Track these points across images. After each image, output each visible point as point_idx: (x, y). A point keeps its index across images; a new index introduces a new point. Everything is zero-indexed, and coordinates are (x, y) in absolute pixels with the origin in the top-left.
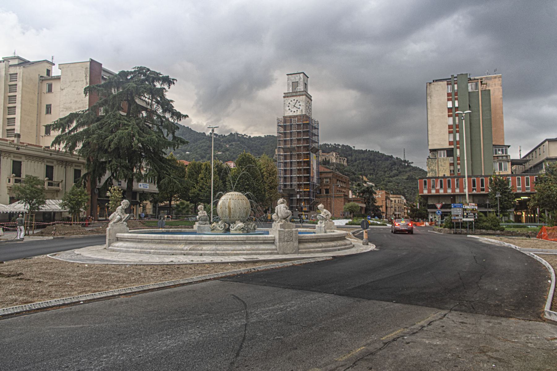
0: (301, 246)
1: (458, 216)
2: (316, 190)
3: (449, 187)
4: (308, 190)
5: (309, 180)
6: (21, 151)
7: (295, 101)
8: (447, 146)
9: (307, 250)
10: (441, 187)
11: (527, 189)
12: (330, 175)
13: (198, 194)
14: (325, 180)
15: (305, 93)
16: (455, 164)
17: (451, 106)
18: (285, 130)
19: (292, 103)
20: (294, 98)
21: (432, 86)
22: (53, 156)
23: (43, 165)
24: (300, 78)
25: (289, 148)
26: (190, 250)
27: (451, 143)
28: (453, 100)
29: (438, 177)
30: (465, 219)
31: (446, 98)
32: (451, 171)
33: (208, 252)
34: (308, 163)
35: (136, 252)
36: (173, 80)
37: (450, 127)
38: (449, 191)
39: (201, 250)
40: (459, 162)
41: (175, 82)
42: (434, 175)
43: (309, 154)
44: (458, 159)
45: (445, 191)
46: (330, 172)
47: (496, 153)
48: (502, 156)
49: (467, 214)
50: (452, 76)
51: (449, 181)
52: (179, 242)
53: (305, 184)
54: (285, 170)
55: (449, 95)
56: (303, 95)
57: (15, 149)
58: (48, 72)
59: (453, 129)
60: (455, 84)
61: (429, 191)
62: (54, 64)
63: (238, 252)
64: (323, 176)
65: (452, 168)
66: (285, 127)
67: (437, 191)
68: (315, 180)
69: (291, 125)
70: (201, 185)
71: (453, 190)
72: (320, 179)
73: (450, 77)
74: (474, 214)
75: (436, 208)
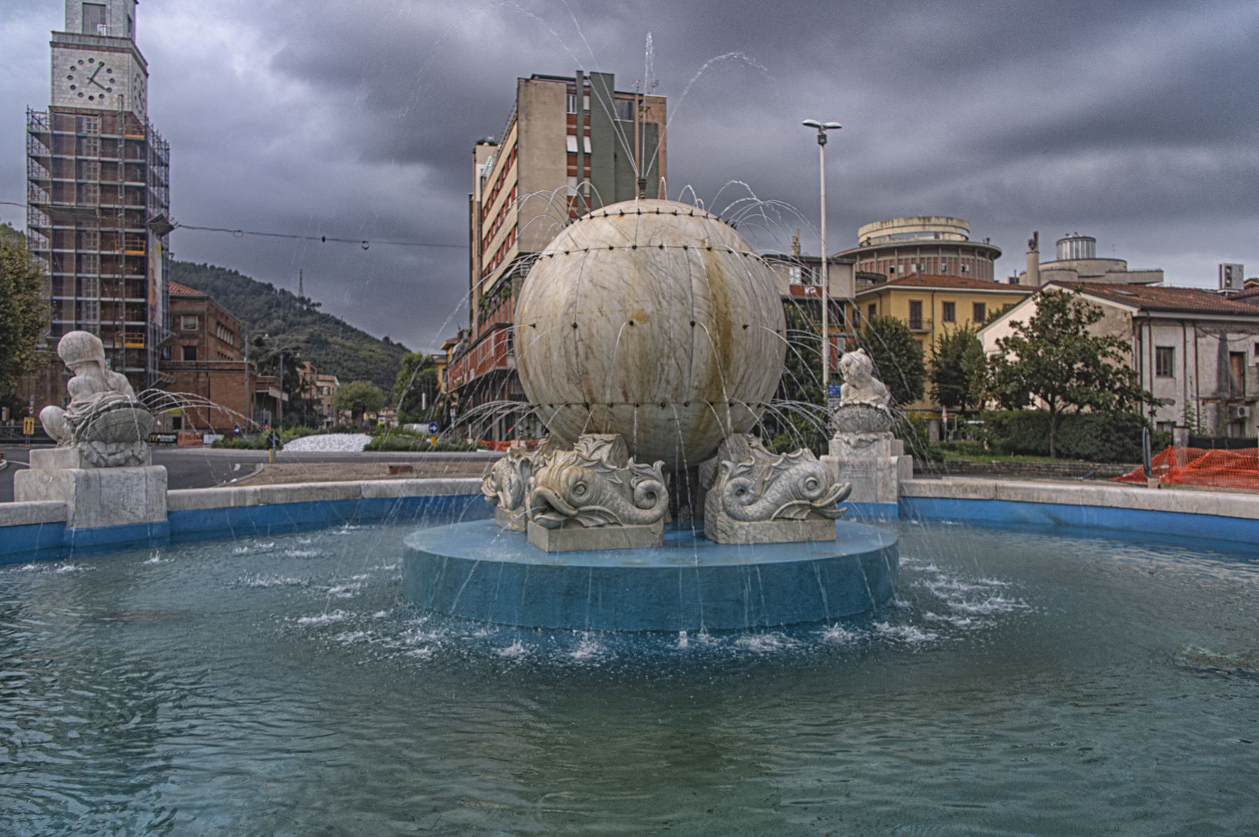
2: (161, 347)
4: (142, 346)
5: (143, 317)
7: (96, 65)
12: (201, 308)
14: (183, 321)
17: (575, 150)
19: (87, 70)
21: (532, 89)
25: (71, 210)
28: (580, 133)
31: (565, 125)
34: (142, 264)
43: (144, 237)
46: (202, 299)
50: (580, 72)
53: (128, 328)
54: (57, 281)
55: (571, 119)
56: (123, 51)
64: (178, 307)
66: (56, 142)
72: (172, 319)
73: (574, 76)
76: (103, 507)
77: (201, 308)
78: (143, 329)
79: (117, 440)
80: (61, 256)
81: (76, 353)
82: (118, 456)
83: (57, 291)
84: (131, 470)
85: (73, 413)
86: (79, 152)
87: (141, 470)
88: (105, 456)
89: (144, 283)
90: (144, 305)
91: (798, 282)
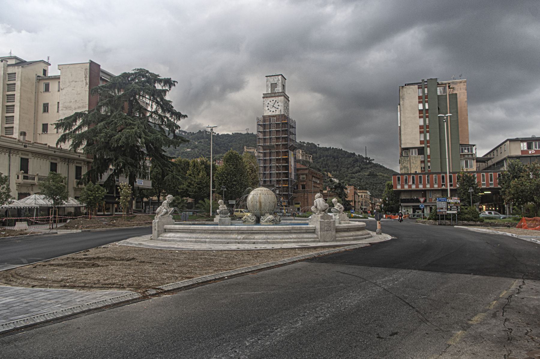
0: (338, 235)
1: (442, 209)
2: (294, 185)
3: (420, 183)
6: (28, 148)
8: (418, 145)
9: (342, 238)
10: (413, 183)
11: (491, 184)
12: (307, 172)
13: (187, 189)
14: (301, 177)
15: (283, 94)
16: (426, 162)
17: (422, 108)
18: (264, 129)
21: (405, 89)
22: (57, 153)
23: (48, 162)
24: (279, 80)
25: (268, 146)
26: (243, 239)
27: (422, 142)
28: (424, 102)
29: (411, 174)
30: (449, 212)
31: (417, 100)
32: (422, 168)
33: (260, 241)
34: (287, 161)
35: (191, 242)
36: (174, 82)
37: (421, 127)
38: (421, 187)
39: (254, 239)
40: (429, 159)
41: (176, 83)
42: (406, 172)
43: (287, 152)
44: (429, 157)
45: (417, 187)
46: (306, 169)
47: (462, 152)
48: (468, 155)
49: (451, 207)
51: (420, 177)
52: (232, 232)
53: (284, 180)
54: (265, 167)
55: (420, 98)
56: (281, 96)
57: (23, 147)
58: (45, 71)
59: (423, 129)
60: (425, 87)
61: (403, 186)
62: (50, 65)
63: (286, 240)
65: (423, 165)
66: (264, 126)
67: (410, 186)
68: (293, 177)
69: (270, 124)
70: (189, 181)
71: (424, 186)
72: (297, 176)
73: (421, 81)
74: (457, 207)
75: (420, 202)
77: (307, 172)
78: (287, 180)
80: (266, 160)
83: (265, 171)
86: (270, 128)
89: (288, 166)
90: (288, 173)
91: (526, 148)
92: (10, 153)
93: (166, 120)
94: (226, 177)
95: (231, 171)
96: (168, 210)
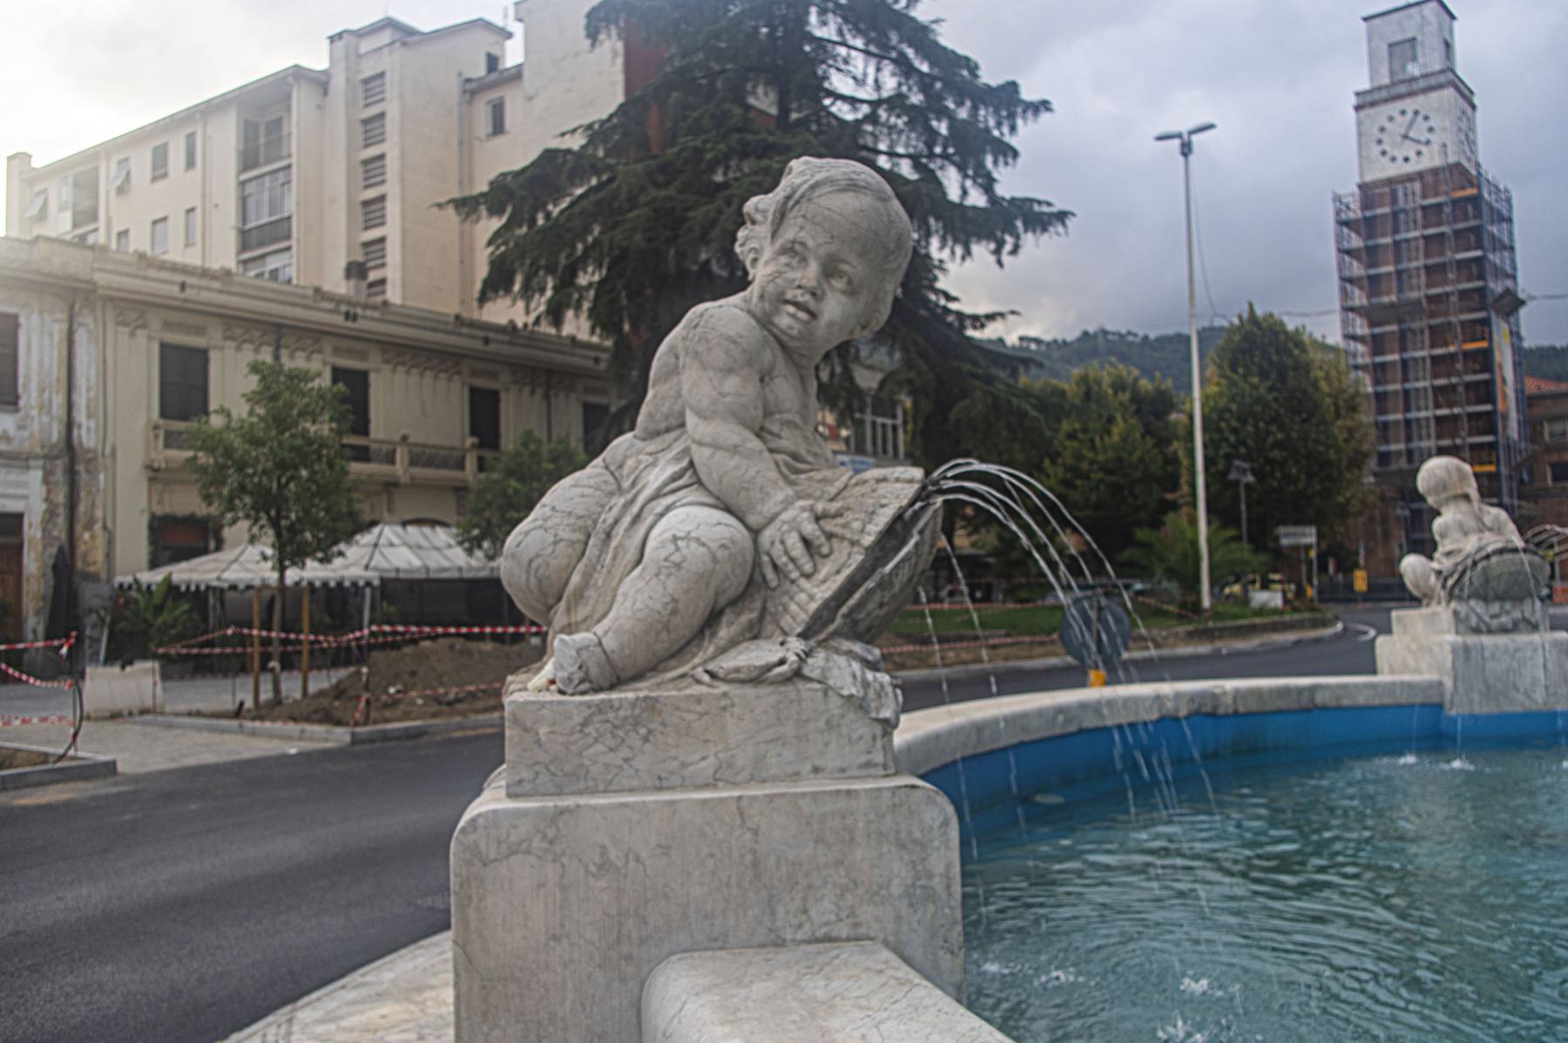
2: (1518, 468)
4: (1492, 468)
5: (1492, 430)
6: (361, 324)
7: (1410, 115)
14: (1547, 428)
15: (1450, 76)
18: (1370, 235)
20: (1400, 105)
22: (493, 347)
23: (456, 384)
25: (1392, 306)
34: (1484, 360)
43: (1486, 322)
54: (1381, 398)
56: (1440, 87)
57: (339, 320)
58: (493, 62)
62: (510, 36)
64: (1538, 411)
68: (1513, 430)
69: (1395, 214)
70: (1069, 461)
72: (1531, 427)
76: (1488, 687)
78: (1492, 446)
79: (1500, 598)
80: (1383, 366)
81: (1441, 487)
82: (1504, 619)
83: (1382, 410)
84: (1523, 638)
85: (1441, 563)
87: (1536, 638)
88: (1487, 619)
89: (1489, 384)
92: (278, 348)
93: (943, 128)
94: (1235, 431)
95: (1258, 400)
96: (789, 519)
